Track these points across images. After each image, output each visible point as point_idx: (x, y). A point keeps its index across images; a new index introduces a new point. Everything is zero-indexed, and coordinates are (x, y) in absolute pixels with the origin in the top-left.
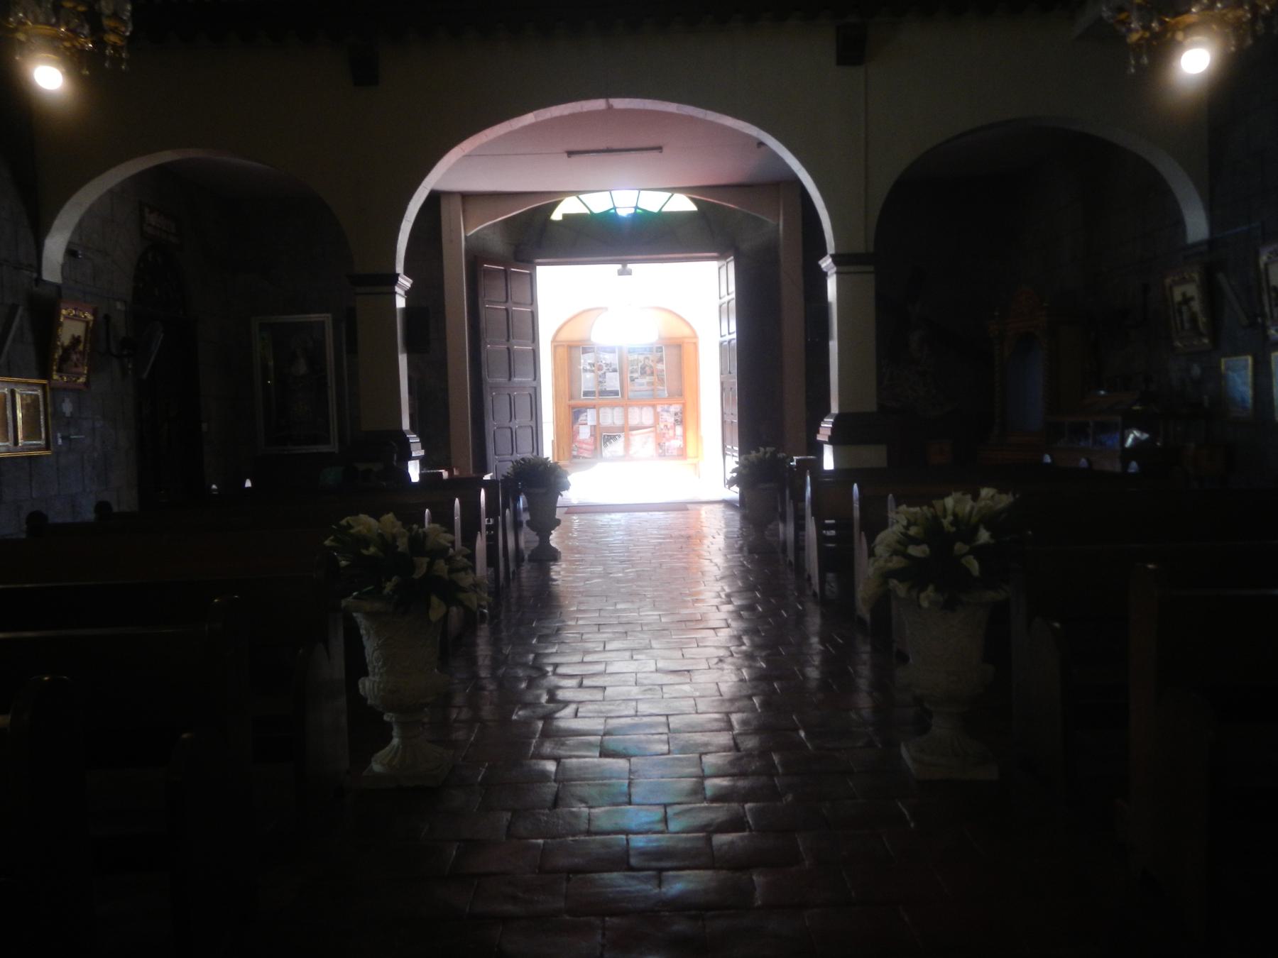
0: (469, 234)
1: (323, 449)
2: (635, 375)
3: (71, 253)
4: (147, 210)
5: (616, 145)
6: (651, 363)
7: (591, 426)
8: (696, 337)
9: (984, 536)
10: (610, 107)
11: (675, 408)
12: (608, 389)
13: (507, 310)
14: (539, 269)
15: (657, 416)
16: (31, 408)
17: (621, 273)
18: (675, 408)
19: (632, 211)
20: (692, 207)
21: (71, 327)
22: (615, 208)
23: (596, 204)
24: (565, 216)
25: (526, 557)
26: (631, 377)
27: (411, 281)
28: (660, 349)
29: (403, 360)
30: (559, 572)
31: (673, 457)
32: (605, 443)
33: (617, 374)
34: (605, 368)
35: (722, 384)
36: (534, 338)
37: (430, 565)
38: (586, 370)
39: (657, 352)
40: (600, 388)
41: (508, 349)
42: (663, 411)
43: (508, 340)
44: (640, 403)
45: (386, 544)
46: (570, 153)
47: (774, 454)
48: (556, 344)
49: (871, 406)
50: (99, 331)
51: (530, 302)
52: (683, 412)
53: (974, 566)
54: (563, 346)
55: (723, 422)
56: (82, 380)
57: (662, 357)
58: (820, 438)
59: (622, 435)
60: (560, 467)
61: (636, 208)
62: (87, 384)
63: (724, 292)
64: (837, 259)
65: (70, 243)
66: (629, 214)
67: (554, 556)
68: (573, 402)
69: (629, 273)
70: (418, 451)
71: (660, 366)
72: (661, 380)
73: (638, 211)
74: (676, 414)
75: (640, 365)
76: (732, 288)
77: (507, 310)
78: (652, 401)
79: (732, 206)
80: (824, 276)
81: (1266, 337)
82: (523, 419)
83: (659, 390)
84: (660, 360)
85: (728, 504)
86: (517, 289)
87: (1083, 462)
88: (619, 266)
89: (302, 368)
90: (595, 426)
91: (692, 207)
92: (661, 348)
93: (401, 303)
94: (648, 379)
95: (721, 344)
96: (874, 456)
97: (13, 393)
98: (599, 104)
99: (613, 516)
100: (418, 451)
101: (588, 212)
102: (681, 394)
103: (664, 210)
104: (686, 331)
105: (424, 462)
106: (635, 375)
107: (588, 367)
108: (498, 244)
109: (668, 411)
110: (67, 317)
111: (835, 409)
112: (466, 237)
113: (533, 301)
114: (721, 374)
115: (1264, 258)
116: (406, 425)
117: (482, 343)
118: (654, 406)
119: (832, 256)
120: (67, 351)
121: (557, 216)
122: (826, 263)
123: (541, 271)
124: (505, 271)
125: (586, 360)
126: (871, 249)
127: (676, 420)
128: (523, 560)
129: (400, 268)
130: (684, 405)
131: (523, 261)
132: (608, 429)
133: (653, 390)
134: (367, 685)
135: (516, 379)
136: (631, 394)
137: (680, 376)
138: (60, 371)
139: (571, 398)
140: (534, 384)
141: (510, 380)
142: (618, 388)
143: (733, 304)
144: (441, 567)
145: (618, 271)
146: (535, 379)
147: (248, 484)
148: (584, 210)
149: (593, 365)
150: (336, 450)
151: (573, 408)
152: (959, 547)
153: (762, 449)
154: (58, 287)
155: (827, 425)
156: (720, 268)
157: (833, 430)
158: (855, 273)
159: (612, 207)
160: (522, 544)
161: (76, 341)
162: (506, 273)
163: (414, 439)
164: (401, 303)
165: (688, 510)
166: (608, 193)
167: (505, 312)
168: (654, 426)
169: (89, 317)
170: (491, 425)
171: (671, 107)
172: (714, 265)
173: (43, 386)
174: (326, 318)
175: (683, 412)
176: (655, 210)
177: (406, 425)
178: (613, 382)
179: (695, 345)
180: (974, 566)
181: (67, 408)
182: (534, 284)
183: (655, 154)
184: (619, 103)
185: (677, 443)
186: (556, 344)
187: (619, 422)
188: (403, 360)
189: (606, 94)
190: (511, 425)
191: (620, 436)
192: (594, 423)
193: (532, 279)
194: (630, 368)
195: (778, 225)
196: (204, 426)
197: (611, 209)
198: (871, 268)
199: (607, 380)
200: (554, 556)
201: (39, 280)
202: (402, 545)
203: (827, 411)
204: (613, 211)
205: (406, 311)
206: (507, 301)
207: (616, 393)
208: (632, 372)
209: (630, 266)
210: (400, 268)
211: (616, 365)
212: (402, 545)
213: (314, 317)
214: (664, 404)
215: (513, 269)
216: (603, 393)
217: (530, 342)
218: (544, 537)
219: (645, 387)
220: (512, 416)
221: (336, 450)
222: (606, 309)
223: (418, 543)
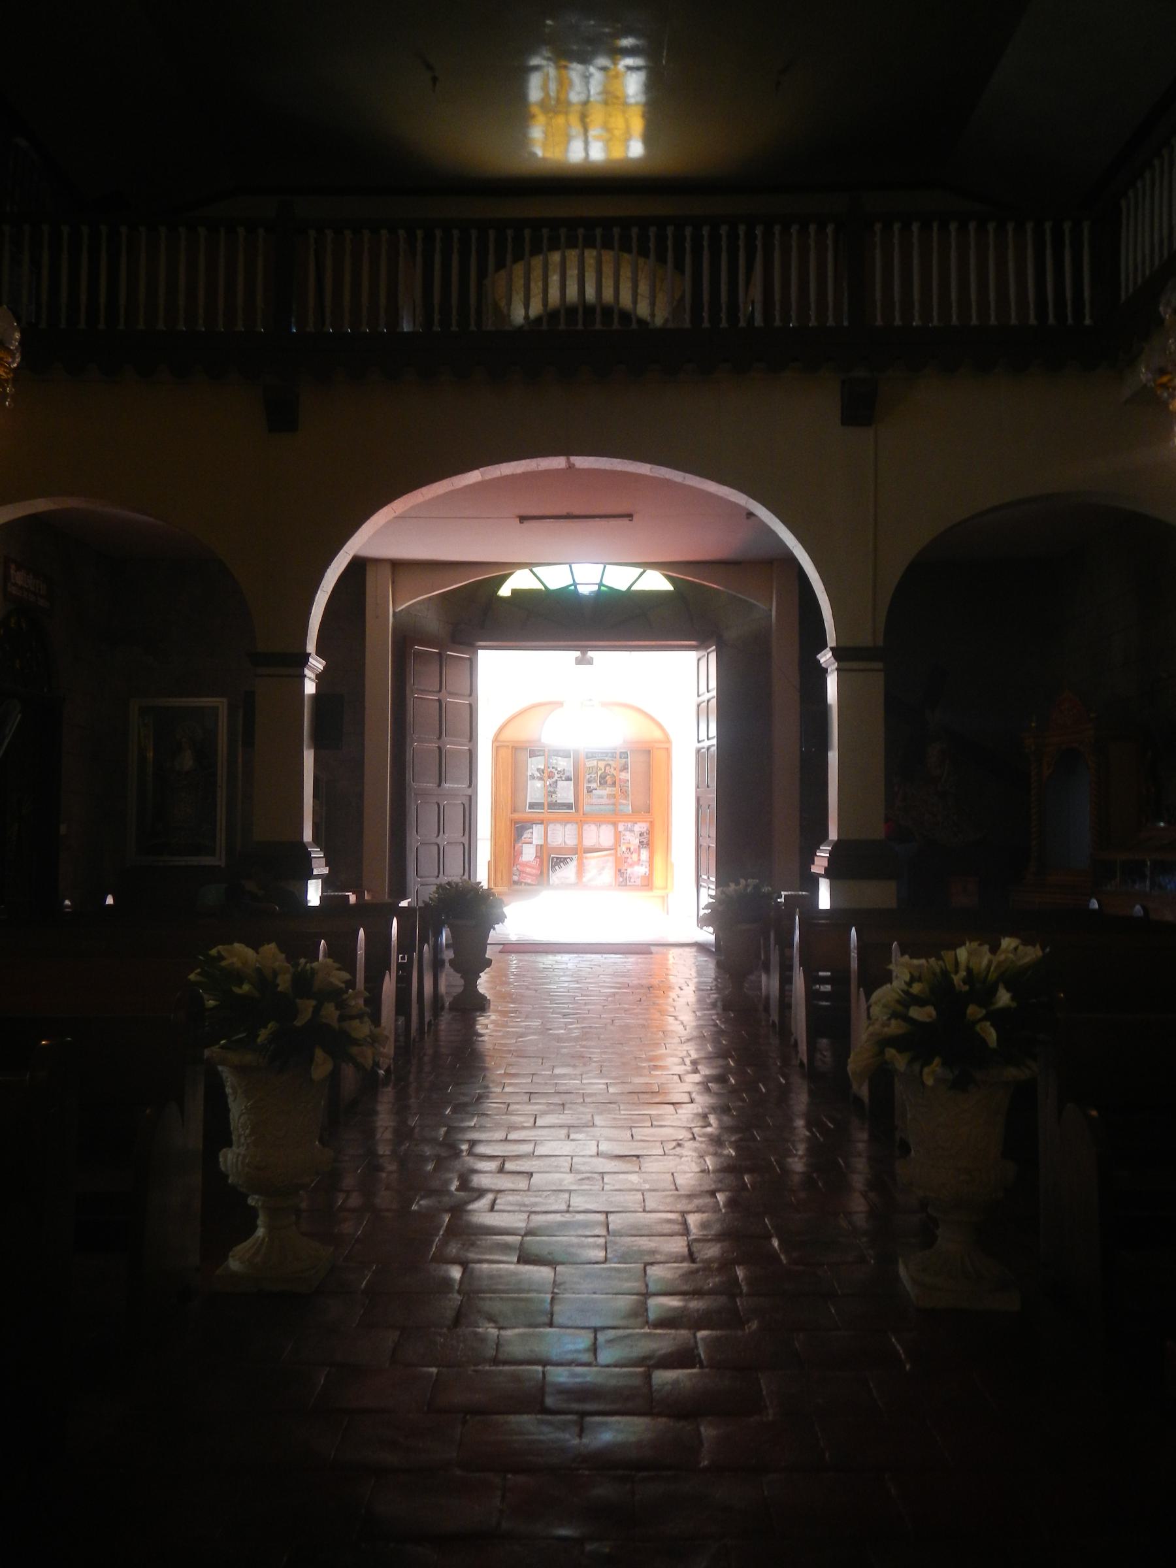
1: (207, 861)
2: (593, 785)
4: (13, 566)
5: (576, 512)
6: (615, 773)
7: (536, 845)
8: (668, 740)
9: (1004, 998)
10: (571, 467)
11: (640, 827)
13: (439, 701)
14: (481, 653)
15: (618, 836)
17: (579, 662)
18: (640, 827)
19: (595, 588)
20: (667, 586)
22: (575, 584)
23: (554, 578)
24: (514, 592)
25: (447, 1004)
26: (588, 788)
27: (324, 662)
28: (624, 755)
29: (309, 757)
30: (487, 1025)
31: (636, 888)
32: (553, 867)
34: (557, 776)
35: (698, 800)
36: (472, 736)
37: (317, 1010)
38: (532, 777)
39: (621, 758)
40: (549, 799)
41: (439, 748)
42: (626, 830)
43: (440, 737)
44: (599, 819)
45: (264, 980)
46: (523, 519)
47: (757, 887)
48: (497, 744)
49: (878, 832)
51: (468, 692)
52: (650, 832)
53: (991, 1036)
54: (508, 746)
57: (626, 764)
58: (815, 869)
60: (493, 895)
61: (600, 584)
63: (703, 688)
64: (837, 653)
66: (592, 592)
67: (480, 1004)
68: (516, 816)
69: (590, 662)
70: (320, 869)
71: (624, 776)
72: (625, 793)
73: (603, 588)
75: (599, 773)
76: (713, 684)
77: (439, 701)
78: (612, 818)
79: (715, 586)
80: (823, 672)
82: (454, 833)
83: (623, 804)
85: (701, 947)
87: (1138, 910)
88: (578, 654)
89: (187, 761)
90: (541, 845)
91: (667, 586)
92: (626, 753)
93: (310, 688)
94: (608, 791)
95: (698, 751)
98: (557, 463)
99: (559, 957)
100: (320, 869)
101: (543, 588)
102: (648, 810)
103: (633, 588)
104: (658, 734)
105: (327, 882)
106: (593, 785)
107: (537, 774)
108: (432, 623)
109: (632, 831)
111: (833, 835)
113: (472, 691)
114: (698, 787)
116: (308, 836)
117: (408, 739)
118: (615, 824)
119: (832, 649)
121: (505, 591)
122: (825, 658)
123: (481, 653)
124: (440, 654)
125: (534, 765)
126: (881, 643)
128: (443, 1008)
129: (311, 647)
130: (651, 822)
131: (460, 644)
132: (558, 850)
133: (614, 804)
134: (229, 1159)
136: (587, 808)
137: (649, 790)
139: (514, 810)
140: (469, 792)
141: (439, 785)
142: (572, 800)
143: (714, 702)
144: (330, 1012)
145: (576, 659)
146: (470, 786)
147: (110, 900)
148: (537, 586)
149: (541, 771)
151: (516, 823)
152: (974, 1011)
153: (743, 881)
155: (823, 855)
156: (699, 660)
157: (830, 860)
158: (862, 670)
159: (572, 582)
160: (442, 989)
163: (316, 853)
164: (310, 688)
165: (651, 953)
166: (568, 566)
167: (438, 704)
168: (614, 848)
170: (414, 840)
171: (644, 469)
172: (692, 655)
174: (220, 703)
175: (650, 832)
176: (624, 588)
177: (308, 836)
178: (565, 793)
179: (668, 751)
180: (991, 1036)
182: (474, 673)
183: (625, 522)
184: (583, 462)
185: (641, 870)
187: (571, 842)
188: (309, 757)
189: (567, 452)
190: (439, 840)
191: (571, 859)
192: (541, 842)
193: (472, 664)
194: (588, 776)
195: (771, 610)
196: (63, 829)
197: (570, 585)
198: (880, 665)
199: (558, 790)
200: (480, 1004)
202: (284, 983)
203: (823, 837)
204: (573, 588)
205: (316, 698)
206: (440, 691)
207: (569, 806)
208: (589, 782)
209: (590, 654)
210: (311, 647)
211: (570, 771)
212: (284, 983)
214: (627, 822)
215: (448, 653)
216: (553, 805)
218: (471, 977)
219: (605, 801)
220: (440, 829)
222: (559, 704)
223: (303, 983)
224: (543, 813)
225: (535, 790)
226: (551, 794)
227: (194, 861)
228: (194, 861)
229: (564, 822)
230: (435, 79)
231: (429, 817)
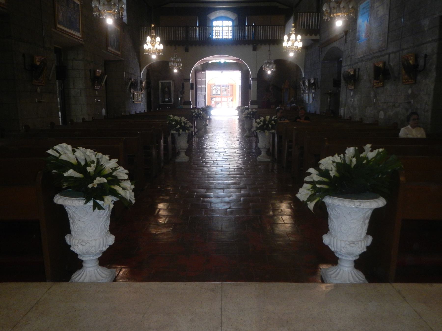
2: (223, 91)
3: (143, 74)
6: (227, 89)
11: (231, 98)
12: (218, 94)
15: (228, 100)
17: (221, 73)
18: (231, 98)
28: (228, 86)
30: (212, 120)
33: (220, 91)
34: (217, 90)
35: (239, 94)
36: (205, 85)
38: (214, 90)
41: (201, 87)
44: (224, 97)
49: (255, 99)
55: (239, 101)
59: (221, 103)
64: (252, 79)
67: (211, 119)
68: (211, 96)
69: (223, 73)
70: (192, 104)
71: (229, 90)
72: (229, 92)
74: (231, 99)
78: (227, 96)
81: (306, 92)
82: (203, 100)
84: (229, 88)
86: (203, 76)
88: (221, 72)
89: (167, 90)
90: (215, 101)
94: (226, 92)
96: (256, 106)
102: (232, 95)
106: (223, 91)
107: (214, 89)
108: (200, 68)
115: (311, 80)
118: (227, 97)
120: (143, 88)
121: (210, 62)
122: (250, 79)
125: (214, 88)
126: (256, 77)
127: (231, 101)
130: (233, 97)
132: (218, 102)
133: (227, 94)
135: (202, 92)
136: (223, 95)
137: (233, 92)
139: (211, 95)
142: (220, 93)
148: (216, 62)
149: (215, 89)
150: (173, 104)
161: (144, 87)
170: (198, 100)
173: (142, 93)
175: (233, 99)
176: (228, 62)
178: (219, 92)
186: (208, 84)
192: (215, 100)
193: (205, 74)
199: (218, 92)
201: (141, 78)
207: (220, 95)
208: (223, 90)
209: (223, 72)
211: (220, 89)
216: (217, 94)
217: (204, 86)
219: (225, 94)
220: (201, 99)
221: (173, 104)
224: (216, 96)
225: (214, 92)
226: (217, 92)
229: (219, 97)
231: (200, 97)
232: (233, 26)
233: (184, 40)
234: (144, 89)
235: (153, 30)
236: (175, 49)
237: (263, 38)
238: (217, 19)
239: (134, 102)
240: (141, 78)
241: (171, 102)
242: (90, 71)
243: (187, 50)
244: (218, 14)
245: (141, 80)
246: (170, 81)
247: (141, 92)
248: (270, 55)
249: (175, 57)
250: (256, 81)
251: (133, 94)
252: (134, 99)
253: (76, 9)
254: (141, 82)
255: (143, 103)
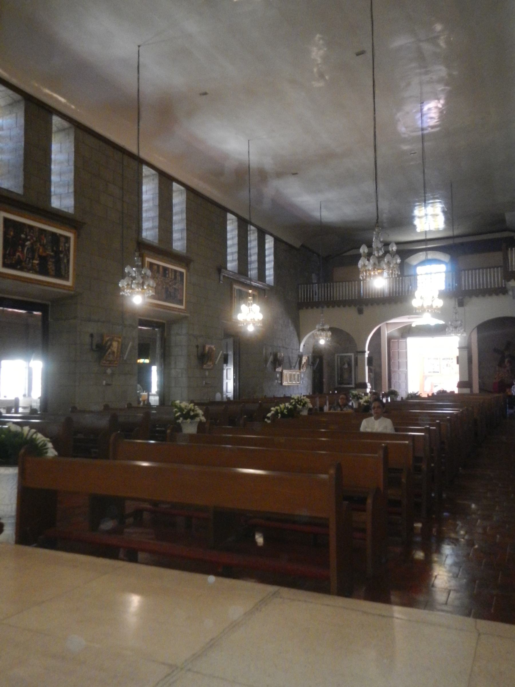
0: (389, 332)
1: (351, 386)
3: (304, 345)
16: (298, 375)
21: (304, 360)
50: (308, 360)
56: (305, 370)
62: (305, 371)
65: (304, 343)
89: (346, 366)
97: (296, 373)
108: (396, 334)
110: (304, 359)
112: (387, 334)
135: (401, 369)
138: (302, 369)
147: (336, 392)
154: (302, 353)
161: (305, 363)
162: (398, 341)
169: (307, 358)
173: (300, 372)
181: (302, 376)
193: (406, 342)
201: (299, 352)
213: (349, 354)
227: (348, 386)
228: (348, 386)
230: (389, 235)
232: (446, 272)
233: (357, 298)
234: (304, 366)
235: (251, 297)
236: (322, 313)
237: (487, 286)
238: (422, 263)
239: (281, 384)
240: (301, 350)
241: (351, 384)
242: (197, 347)
243: (360, 312)
244: (421, 256)
245: (300, 354)
246: (349, 354)
247: (300, 369)
248: (456, 313)
249: (322, 323)
250: (466, 352)
251: (281, 373)
252: (282, 380)
253: (179, 278)
254: (300, 357)
255: (302, 386)
